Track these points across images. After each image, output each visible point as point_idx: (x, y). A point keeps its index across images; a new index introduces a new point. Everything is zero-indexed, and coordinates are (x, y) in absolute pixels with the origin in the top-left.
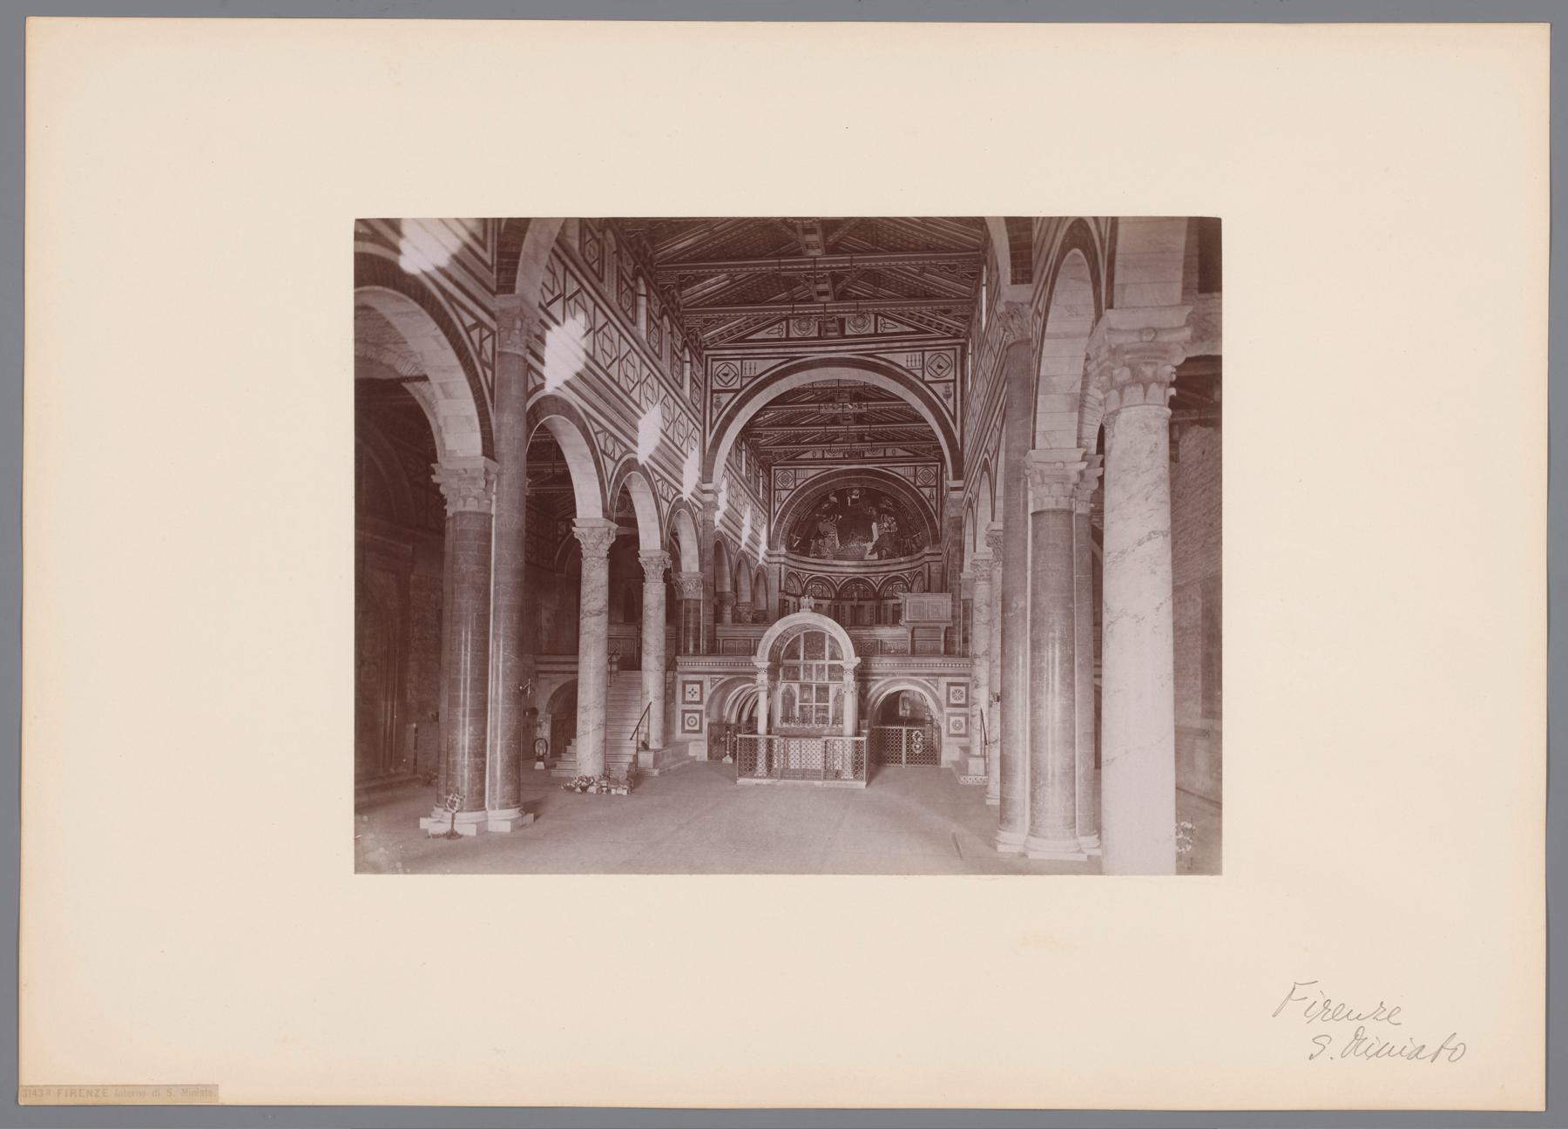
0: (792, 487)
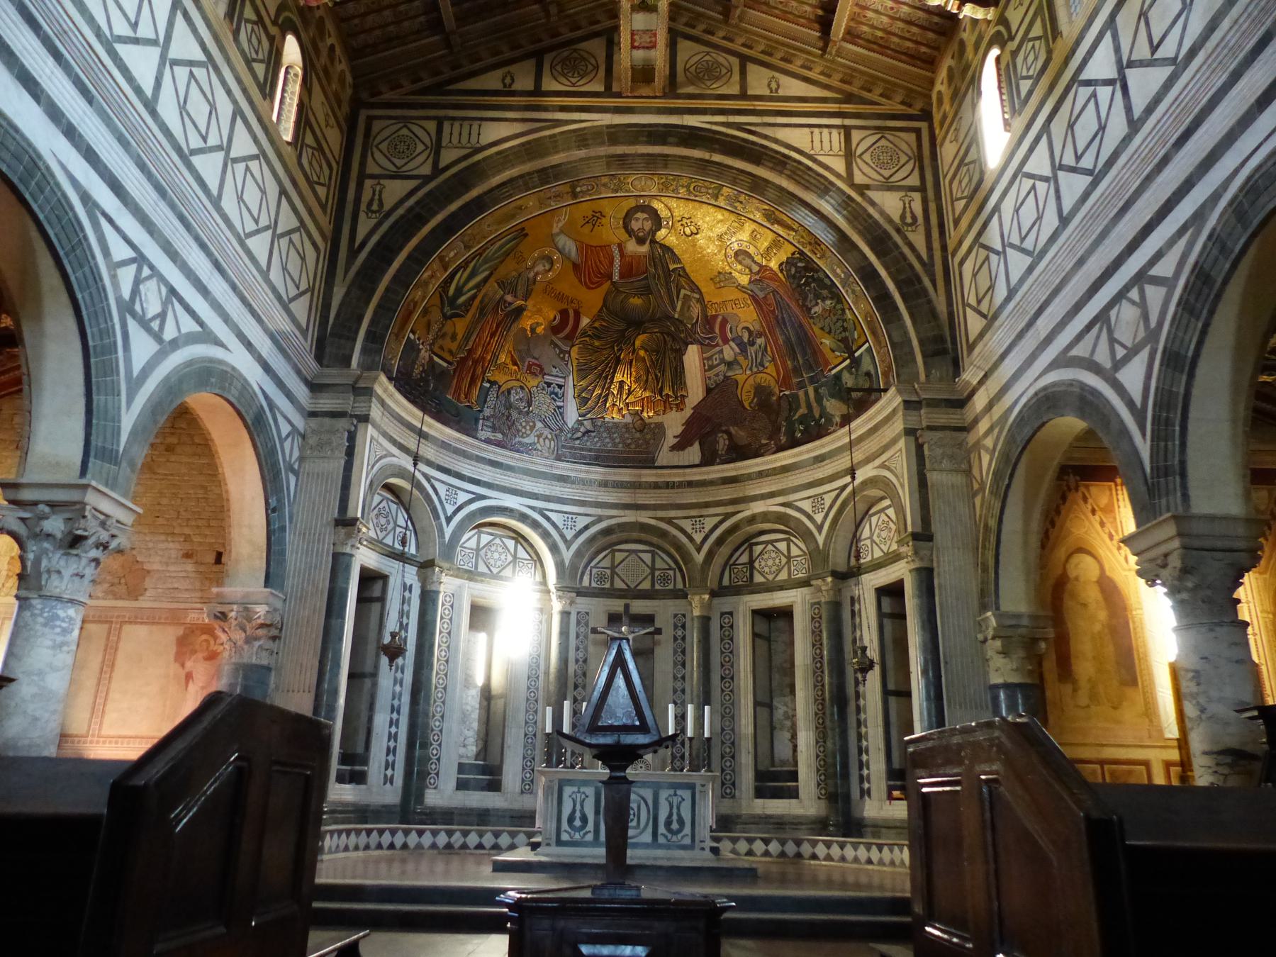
0: (426, 170)
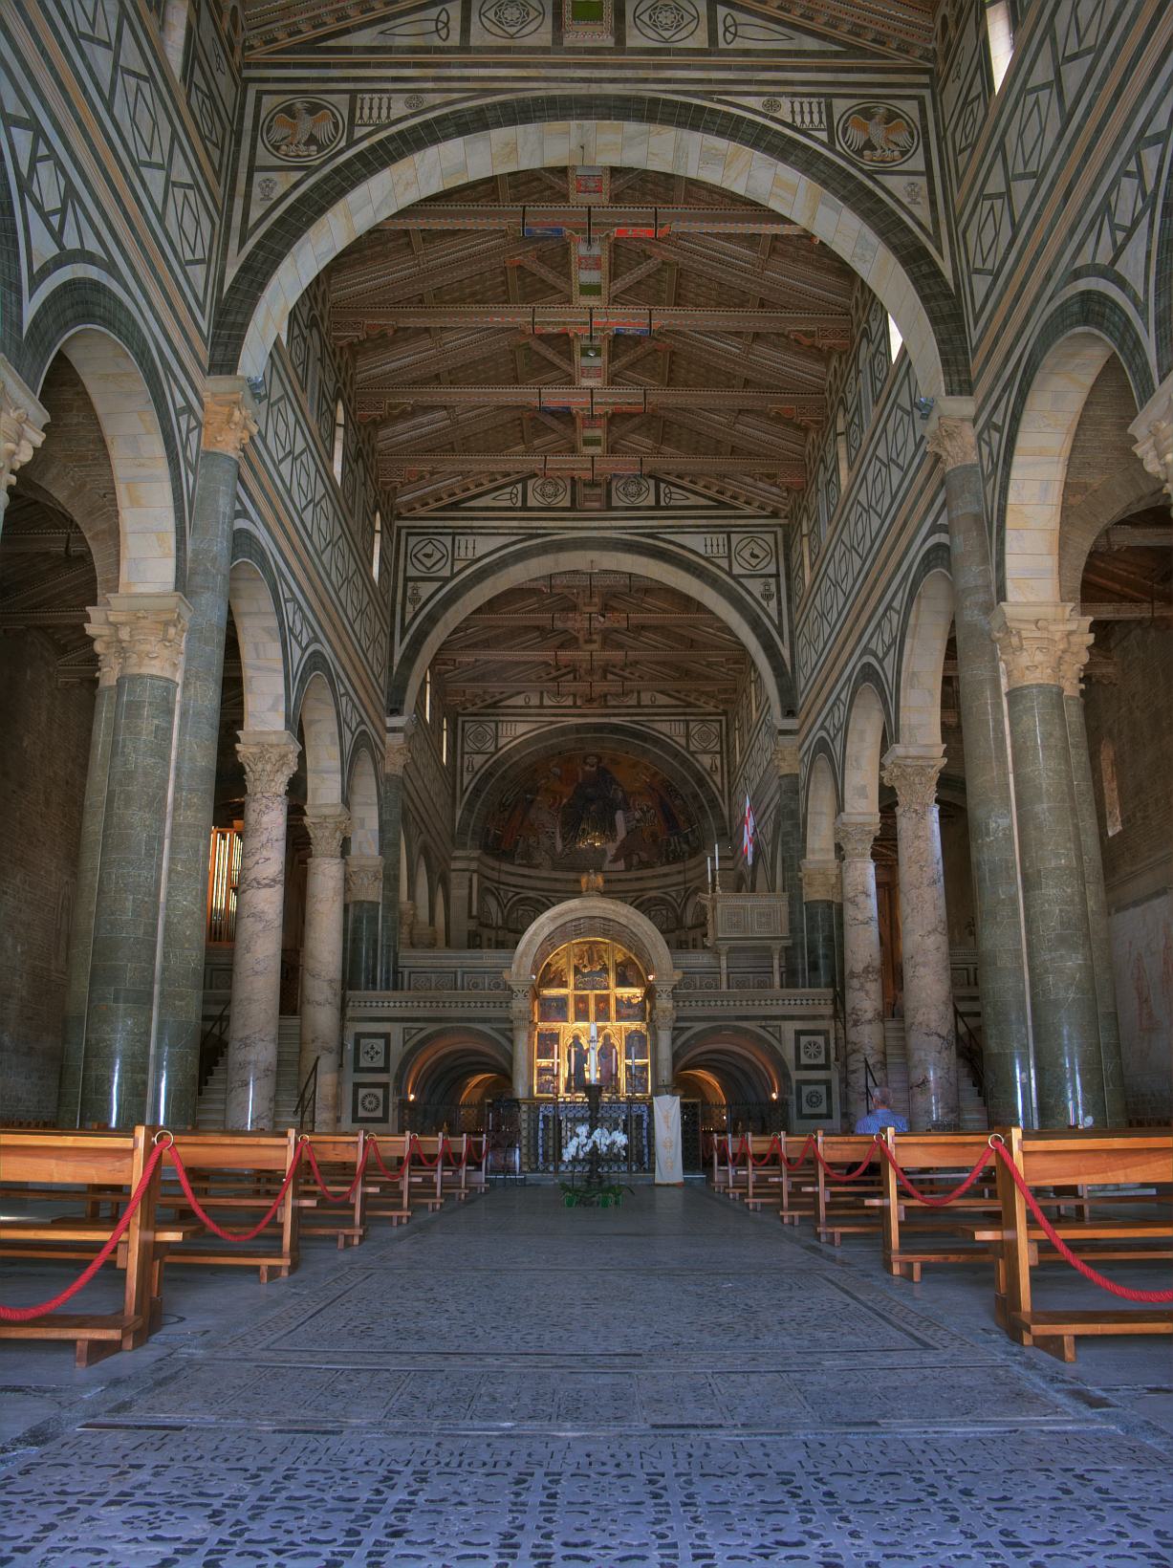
0: (492, 749)
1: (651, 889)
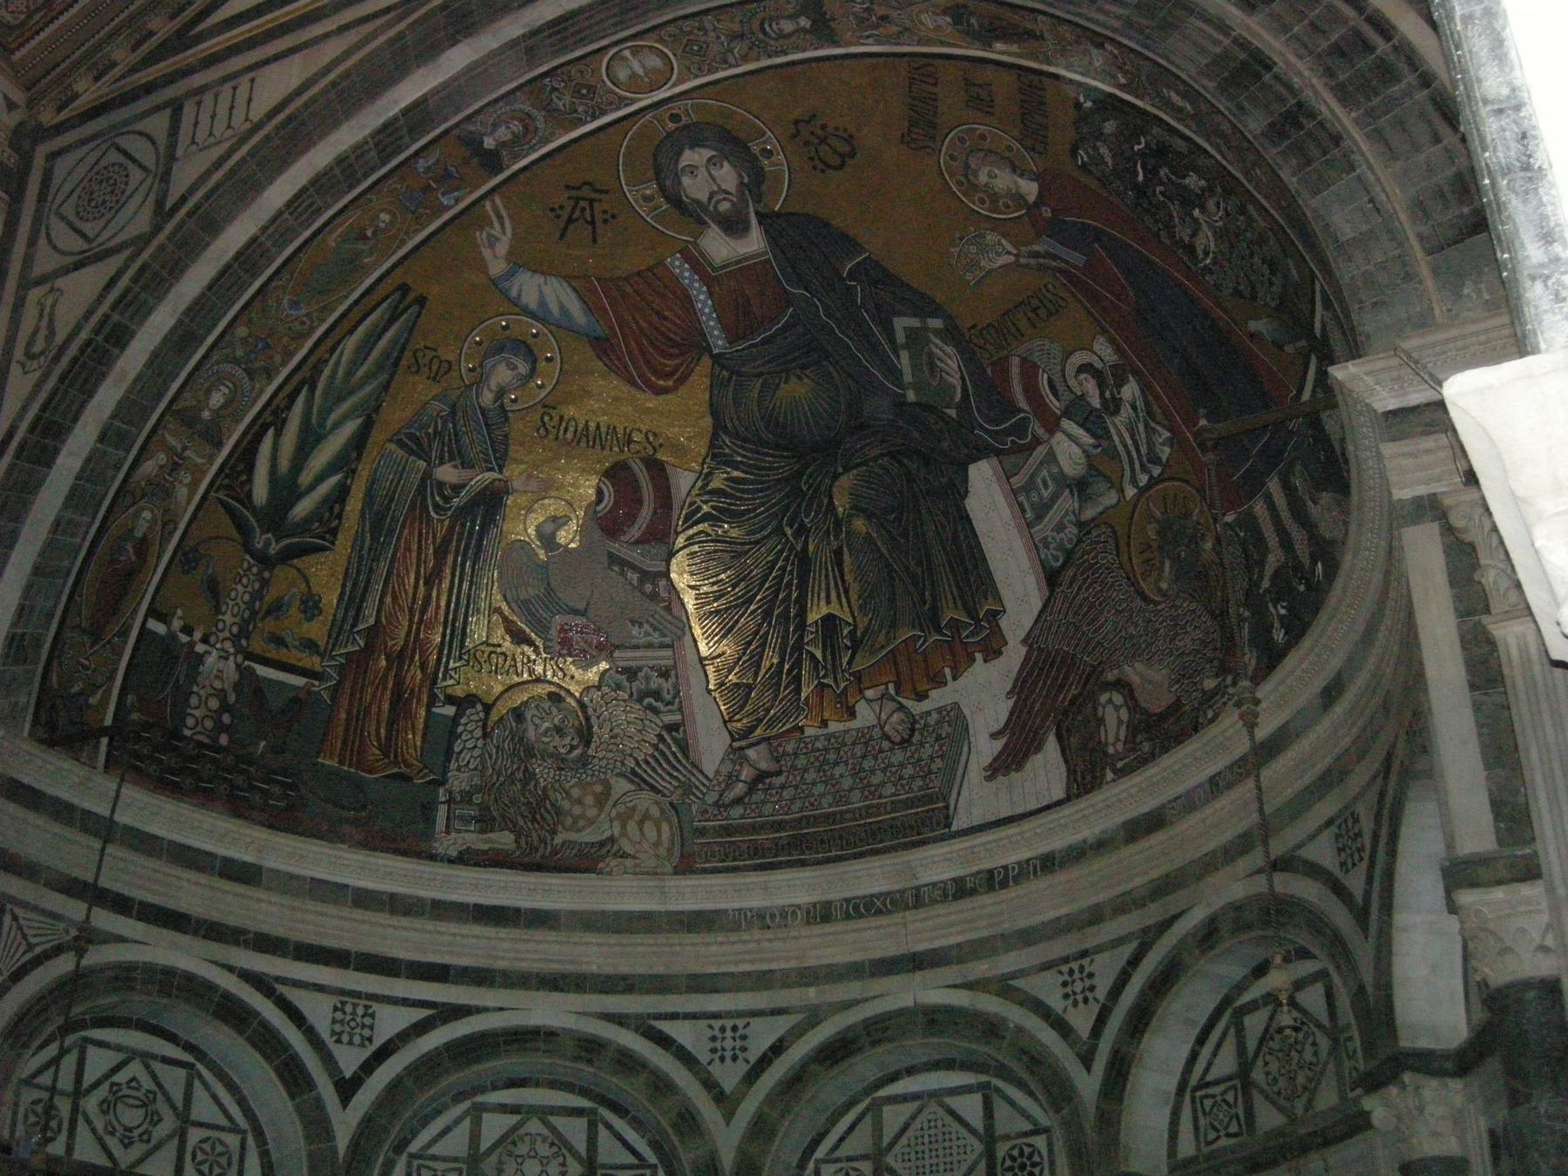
1: (1208, 865)
